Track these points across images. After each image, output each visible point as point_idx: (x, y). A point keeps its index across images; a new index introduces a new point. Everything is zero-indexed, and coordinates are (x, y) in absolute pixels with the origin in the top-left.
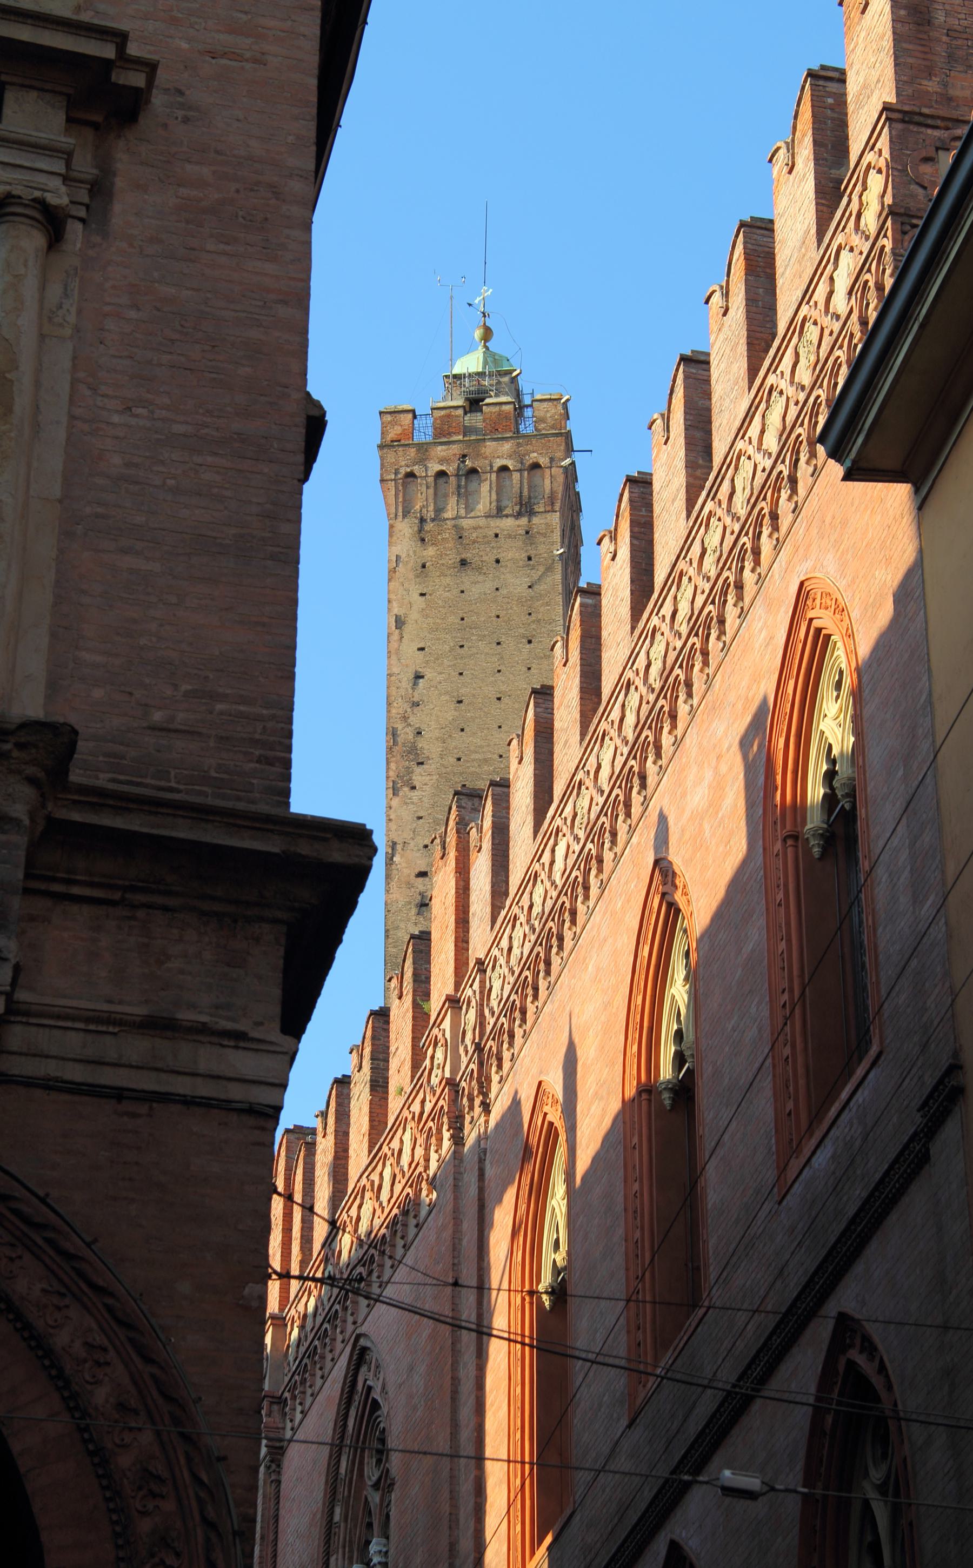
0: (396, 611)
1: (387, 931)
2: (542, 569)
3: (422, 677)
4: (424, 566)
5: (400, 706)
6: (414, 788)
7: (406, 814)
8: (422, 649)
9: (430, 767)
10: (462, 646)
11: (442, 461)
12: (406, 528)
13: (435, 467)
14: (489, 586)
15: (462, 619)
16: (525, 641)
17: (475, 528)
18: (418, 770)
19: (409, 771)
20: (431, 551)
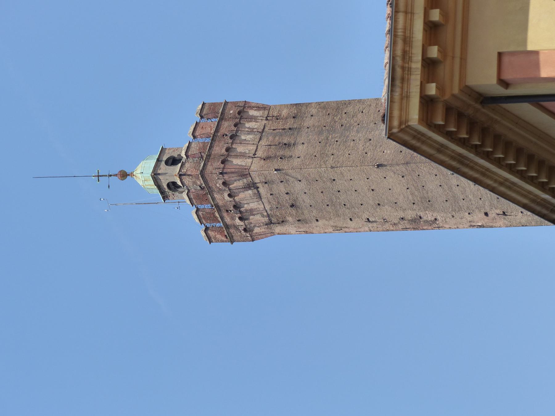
0: (331, 230)
1: (523, 226)
2: (287, 177)
3: (368, 219)
4: (299, 220)
5: (387, 226)
6: (436, 219)
7: (453, 221)
8: (351, 219)
9: (422, 214)
10: (345, 205)
11: (233, 218)
12: (278, 229)
13: (238, 222)
14: (304, 196)
15: (328, 205)
16: (334, 182)
17: (270, 203)
18: (425, 218)
19: (426, 222)
20: (290, 219)
